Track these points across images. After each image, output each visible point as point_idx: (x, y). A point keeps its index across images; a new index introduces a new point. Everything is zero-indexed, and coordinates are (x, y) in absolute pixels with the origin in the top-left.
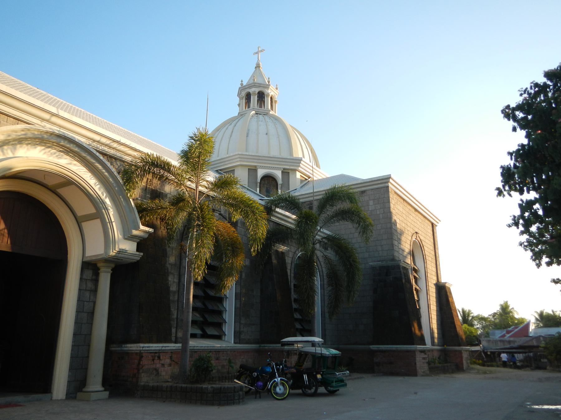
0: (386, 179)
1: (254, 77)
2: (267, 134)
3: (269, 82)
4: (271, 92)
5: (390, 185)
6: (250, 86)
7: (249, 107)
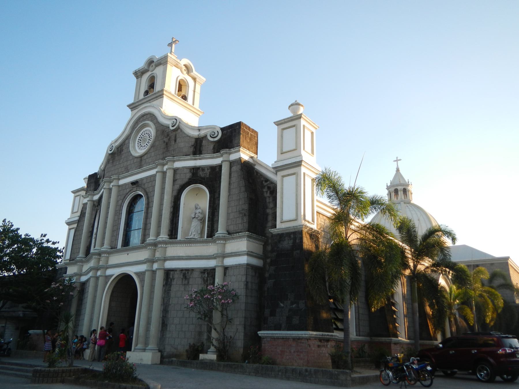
0: (507, 258)
1: (400, 179)
2: (418, 220)
3: (408, 182)
4: (409, 188)
5: (509, 262)
6: (398, 185)
7: (397, 199)
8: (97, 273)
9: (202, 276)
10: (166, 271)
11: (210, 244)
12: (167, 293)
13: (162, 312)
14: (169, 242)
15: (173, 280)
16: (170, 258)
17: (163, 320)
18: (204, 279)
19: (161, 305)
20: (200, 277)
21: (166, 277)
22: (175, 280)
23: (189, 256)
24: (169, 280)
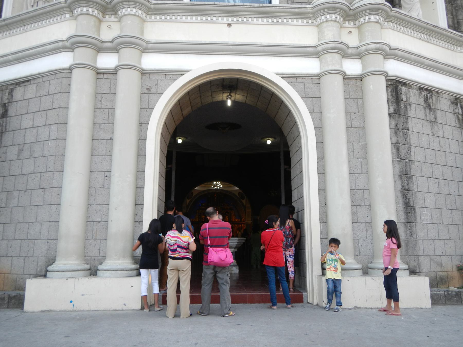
8: (96, 59)
9: (454, 110)
10: (390, 83)
11: (459, 49)
12: (403, 134)
13: (397, 176)
14: (394, 16)
15: (408, 107)
16: (403, 53)
17: (406, 197)
18: (458, 117)
19: (393, 160)
20: (452, 111)
21: (392, 95)
22: (413, 106)
23: (436, 61)
24: (402, 105)
